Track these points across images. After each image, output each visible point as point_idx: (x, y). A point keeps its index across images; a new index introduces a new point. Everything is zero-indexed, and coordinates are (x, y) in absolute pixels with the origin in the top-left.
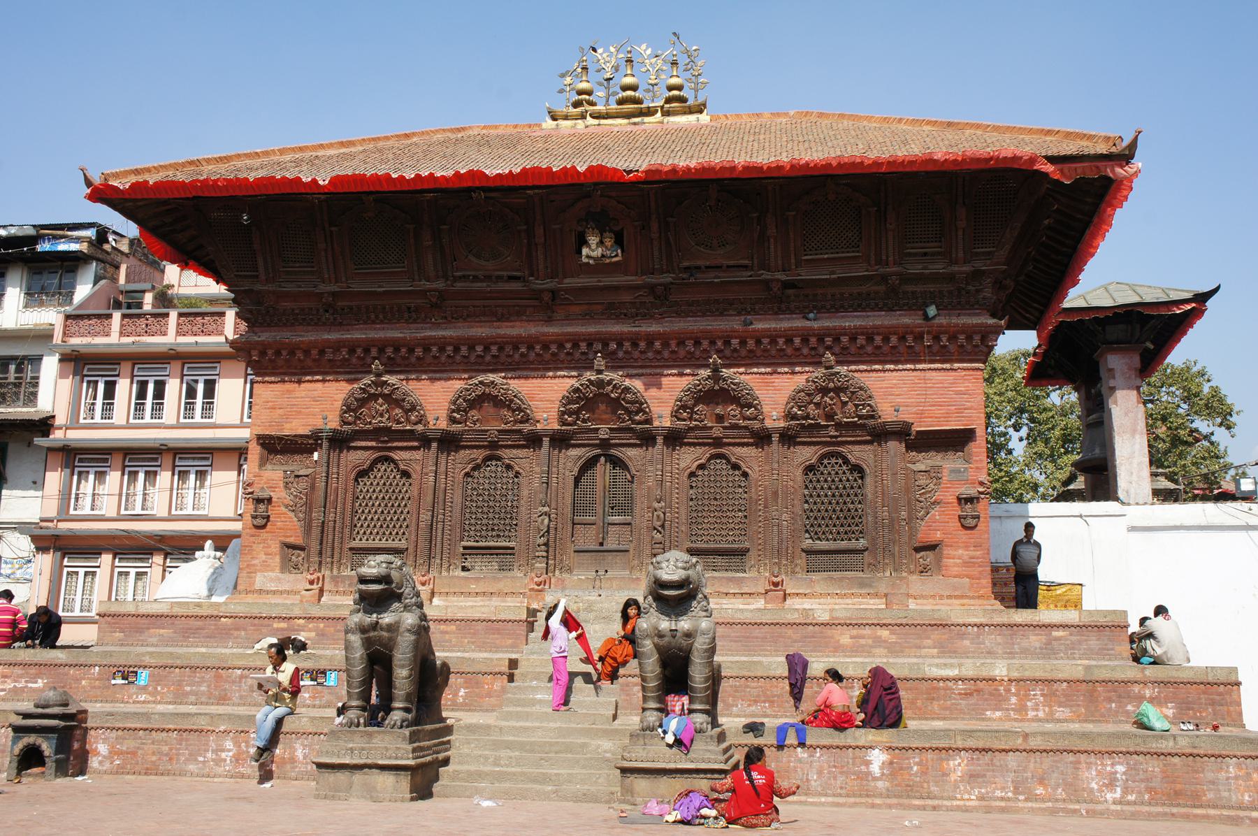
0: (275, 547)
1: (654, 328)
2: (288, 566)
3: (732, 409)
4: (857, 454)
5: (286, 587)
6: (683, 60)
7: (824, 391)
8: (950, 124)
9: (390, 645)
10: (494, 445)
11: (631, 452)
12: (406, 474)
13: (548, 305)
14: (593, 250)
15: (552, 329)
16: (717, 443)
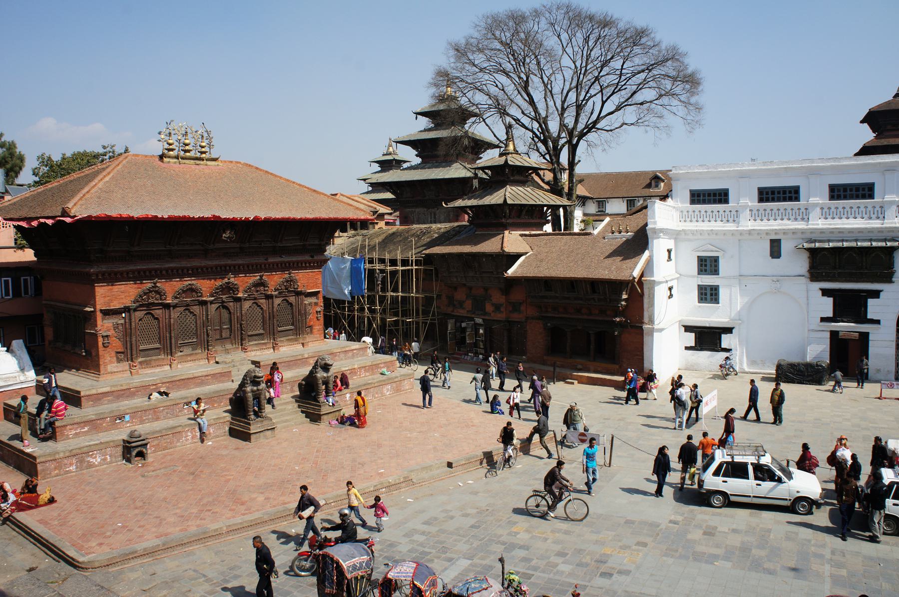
0: (113, 354)
1: (240, 262)
2: (119, 361)
3: (262, 288)
4: (292, 299)
5: (120, 369)
6: (205, 135)
7: (287, 281)
8: (314, 191)
9: (260, 394)
10: (188, 305)
11: (231, 304)
12: (157, 319)
13: (206, 254)
14: (225, 235)
15: (210, 263)
16: (255, 299)
